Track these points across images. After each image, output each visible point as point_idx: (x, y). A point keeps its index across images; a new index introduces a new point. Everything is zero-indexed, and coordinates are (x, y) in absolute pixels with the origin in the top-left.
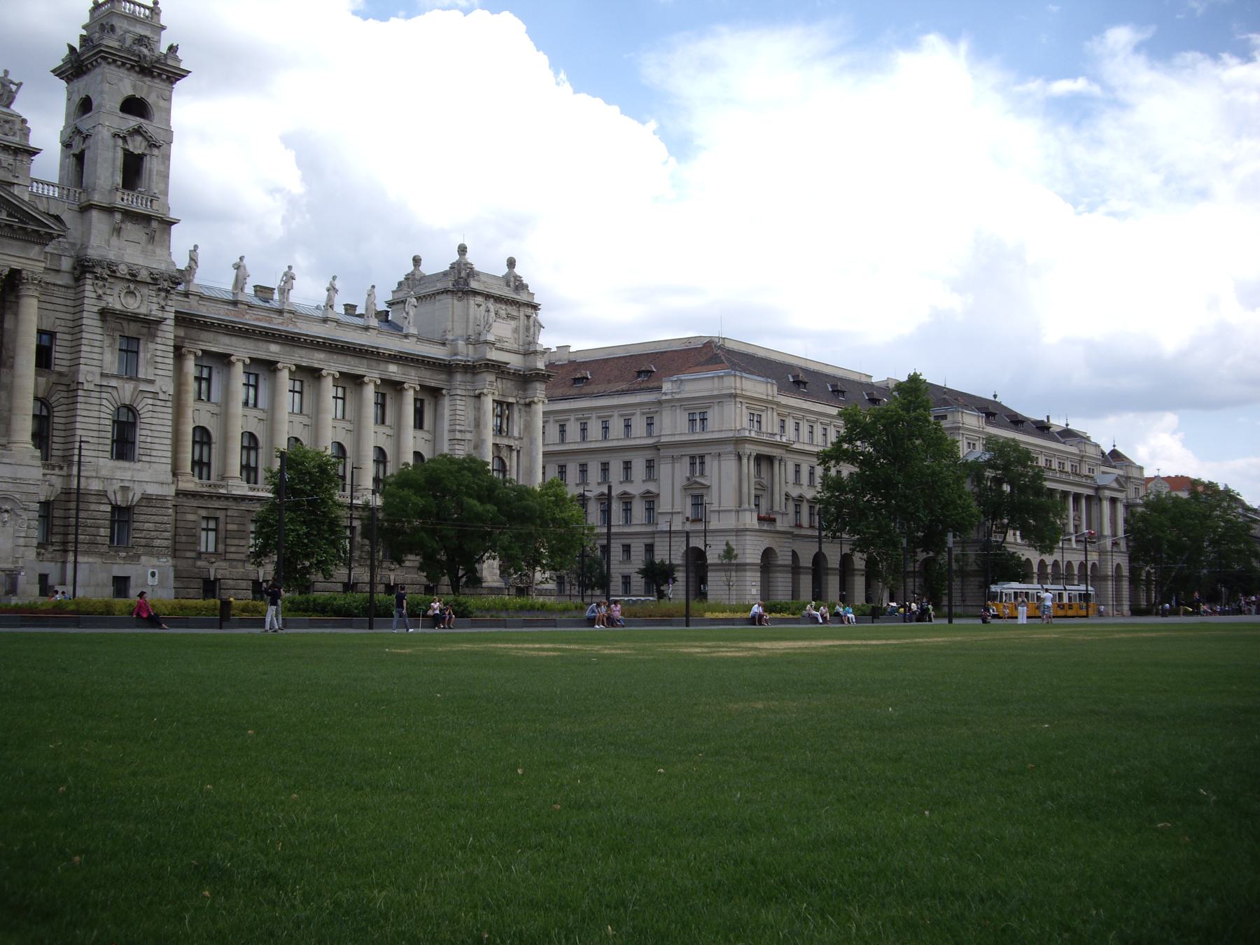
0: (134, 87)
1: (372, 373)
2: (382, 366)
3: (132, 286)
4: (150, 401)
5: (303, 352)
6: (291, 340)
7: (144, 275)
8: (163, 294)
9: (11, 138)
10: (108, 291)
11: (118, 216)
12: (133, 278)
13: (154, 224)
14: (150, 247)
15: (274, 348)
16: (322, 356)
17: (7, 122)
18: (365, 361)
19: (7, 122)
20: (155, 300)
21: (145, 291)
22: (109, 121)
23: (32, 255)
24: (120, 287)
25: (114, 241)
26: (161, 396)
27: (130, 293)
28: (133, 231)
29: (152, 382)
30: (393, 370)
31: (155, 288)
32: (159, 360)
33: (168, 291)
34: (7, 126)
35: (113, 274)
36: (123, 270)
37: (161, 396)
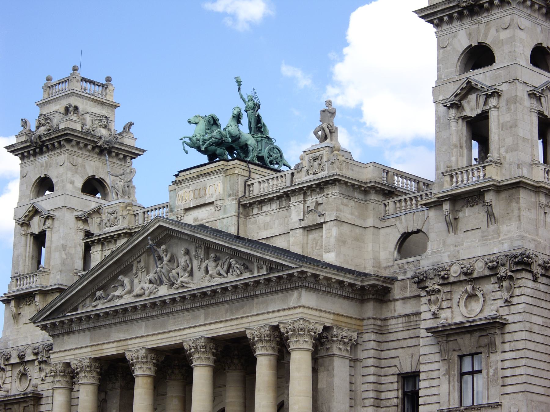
0: (470, 35)
3: (469, 288)
7: (480, 269)
8: (505, 284)
9: (321, 175)
10: (445, 304)
11: (447, 206)
12: (469, 277)
13: (489, 197)
14: (492, 227)
17: (315, 159)
19: (315, 159)
20: (498, 295)
21: (489, 287)
23: (292, 305)
24: (459, 292)
25: (451, 238)
27: (472, 296)
28: (471, 216)
31: (493, 280)
32: (508, 373)
33: (511, 278)
34: (316, 164)
35: (445, 281)
36: (455, 272)
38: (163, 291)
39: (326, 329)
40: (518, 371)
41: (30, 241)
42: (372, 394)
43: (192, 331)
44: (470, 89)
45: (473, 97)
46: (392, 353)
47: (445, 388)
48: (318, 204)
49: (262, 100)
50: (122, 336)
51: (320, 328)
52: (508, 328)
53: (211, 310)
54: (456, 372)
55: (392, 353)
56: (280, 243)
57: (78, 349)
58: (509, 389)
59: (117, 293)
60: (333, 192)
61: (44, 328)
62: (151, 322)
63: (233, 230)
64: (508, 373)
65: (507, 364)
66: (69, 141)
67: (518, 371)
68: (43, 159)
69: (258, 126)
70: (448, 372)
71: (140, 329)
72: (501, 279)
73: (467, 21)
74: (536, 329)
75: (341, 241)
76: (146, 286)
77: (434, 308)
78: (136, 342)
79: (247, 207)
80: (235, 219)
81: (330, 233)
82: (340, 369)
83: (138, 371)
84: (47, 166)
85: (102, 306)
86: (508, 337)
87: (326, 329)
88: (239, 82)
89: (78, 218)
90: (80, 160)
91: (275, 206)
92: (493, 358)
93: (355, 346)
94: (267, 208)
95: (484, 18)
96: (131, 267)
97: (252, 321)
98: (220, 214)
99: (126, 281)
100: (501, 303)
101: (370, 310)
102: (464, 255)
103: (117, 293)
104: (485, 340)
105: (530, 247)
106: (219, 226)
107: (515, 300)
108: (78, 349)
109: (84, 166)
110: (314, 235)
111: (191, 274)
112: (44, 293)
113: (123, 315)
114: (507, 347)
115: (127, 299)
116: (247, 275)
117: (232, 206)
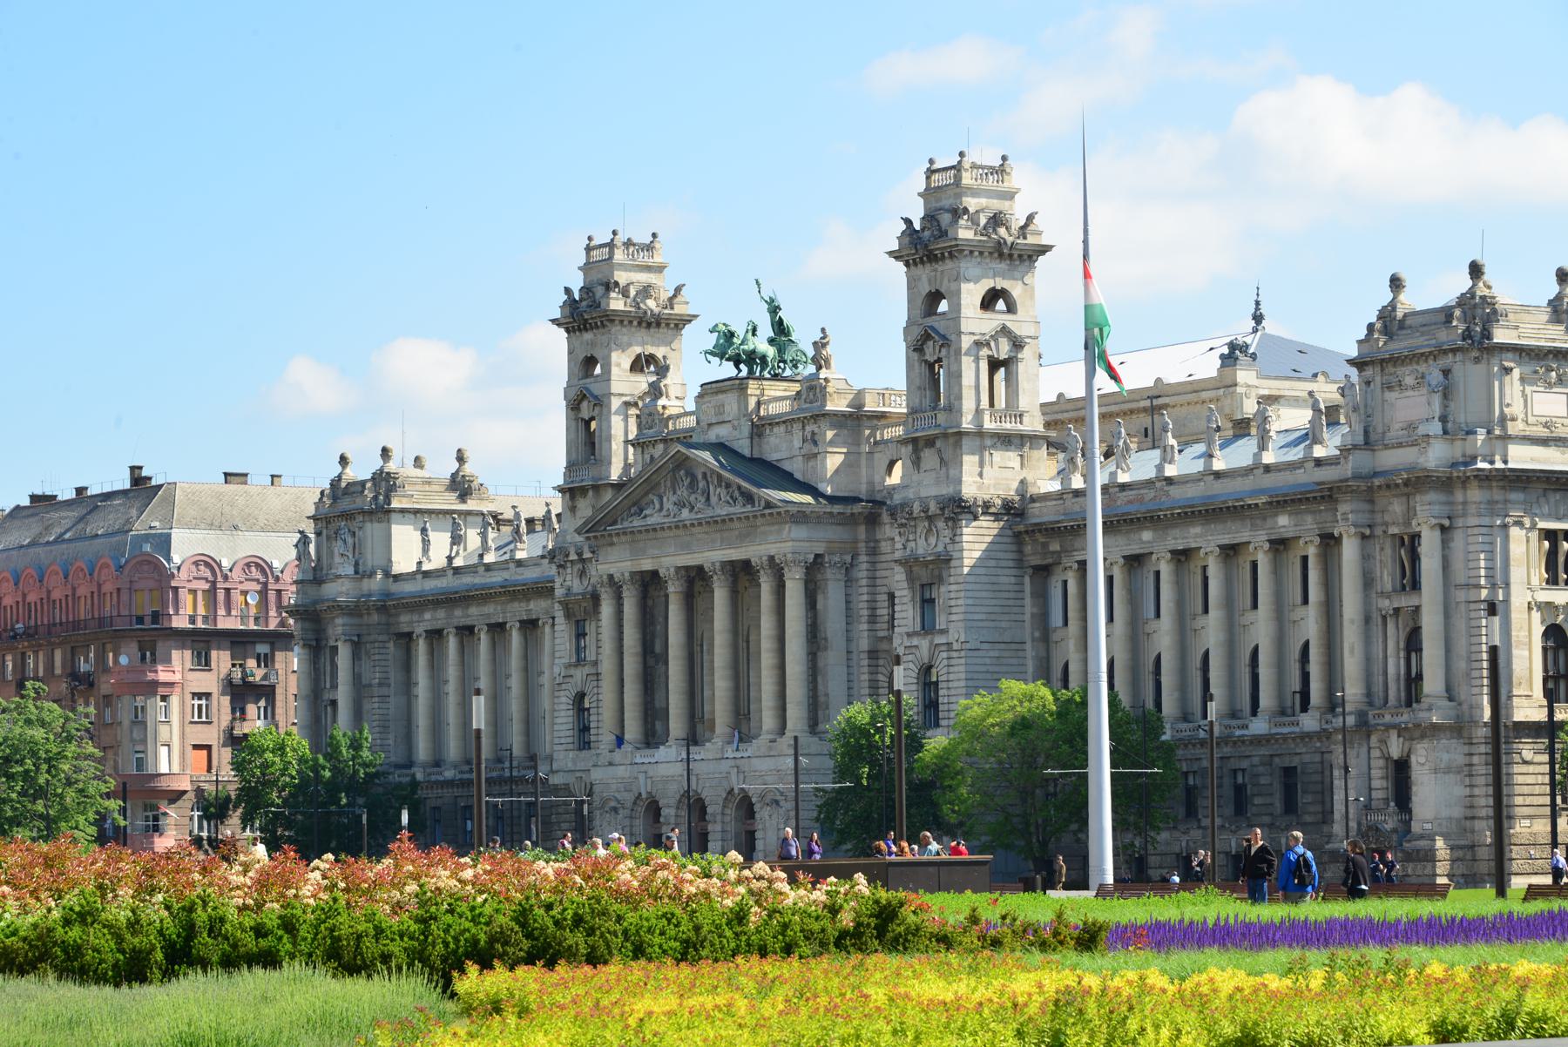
1: (1257, 538)
4: (944, 655)
5: (1176, 532)
6: (1152, 519)
13: (938, 444)
15: (1147, 535)
16: (1197, 530)
18: (1248, 522)
26: (955, 646)
27: (930, 530)
29: (944, 632)
30: (1284, 522)
32: (953, 603)
35: (911, 517)
39: (817, 556)
40: (960, 602)
43: (712, 555)
47: (911, 612)
48: (813, 433)
49: (780, 301)
56: (786, 466)
58: (954, 617)
63: (747, 452)
64: (953, 603)
65: (953, 595)
66: (612, 321)
67: (960, 602)
69: (780, 328)
70: (913, 599)
78: (669, 559)
80: (748, 442)
83: (671, 589)
84: (593, 344)
87: (817, 556)
91: (783, 428)
92: (943, 589)
93: (849, 569)
95: (940, 267)
96: (658, 484)
97: (755, 551)
98: (736, 433)
100: (947, 540)
102: (923, 494)
103: (647, 512)
106: (736, 446)
108: (618, 562)
111: (708, 499)
114: (952, 580)
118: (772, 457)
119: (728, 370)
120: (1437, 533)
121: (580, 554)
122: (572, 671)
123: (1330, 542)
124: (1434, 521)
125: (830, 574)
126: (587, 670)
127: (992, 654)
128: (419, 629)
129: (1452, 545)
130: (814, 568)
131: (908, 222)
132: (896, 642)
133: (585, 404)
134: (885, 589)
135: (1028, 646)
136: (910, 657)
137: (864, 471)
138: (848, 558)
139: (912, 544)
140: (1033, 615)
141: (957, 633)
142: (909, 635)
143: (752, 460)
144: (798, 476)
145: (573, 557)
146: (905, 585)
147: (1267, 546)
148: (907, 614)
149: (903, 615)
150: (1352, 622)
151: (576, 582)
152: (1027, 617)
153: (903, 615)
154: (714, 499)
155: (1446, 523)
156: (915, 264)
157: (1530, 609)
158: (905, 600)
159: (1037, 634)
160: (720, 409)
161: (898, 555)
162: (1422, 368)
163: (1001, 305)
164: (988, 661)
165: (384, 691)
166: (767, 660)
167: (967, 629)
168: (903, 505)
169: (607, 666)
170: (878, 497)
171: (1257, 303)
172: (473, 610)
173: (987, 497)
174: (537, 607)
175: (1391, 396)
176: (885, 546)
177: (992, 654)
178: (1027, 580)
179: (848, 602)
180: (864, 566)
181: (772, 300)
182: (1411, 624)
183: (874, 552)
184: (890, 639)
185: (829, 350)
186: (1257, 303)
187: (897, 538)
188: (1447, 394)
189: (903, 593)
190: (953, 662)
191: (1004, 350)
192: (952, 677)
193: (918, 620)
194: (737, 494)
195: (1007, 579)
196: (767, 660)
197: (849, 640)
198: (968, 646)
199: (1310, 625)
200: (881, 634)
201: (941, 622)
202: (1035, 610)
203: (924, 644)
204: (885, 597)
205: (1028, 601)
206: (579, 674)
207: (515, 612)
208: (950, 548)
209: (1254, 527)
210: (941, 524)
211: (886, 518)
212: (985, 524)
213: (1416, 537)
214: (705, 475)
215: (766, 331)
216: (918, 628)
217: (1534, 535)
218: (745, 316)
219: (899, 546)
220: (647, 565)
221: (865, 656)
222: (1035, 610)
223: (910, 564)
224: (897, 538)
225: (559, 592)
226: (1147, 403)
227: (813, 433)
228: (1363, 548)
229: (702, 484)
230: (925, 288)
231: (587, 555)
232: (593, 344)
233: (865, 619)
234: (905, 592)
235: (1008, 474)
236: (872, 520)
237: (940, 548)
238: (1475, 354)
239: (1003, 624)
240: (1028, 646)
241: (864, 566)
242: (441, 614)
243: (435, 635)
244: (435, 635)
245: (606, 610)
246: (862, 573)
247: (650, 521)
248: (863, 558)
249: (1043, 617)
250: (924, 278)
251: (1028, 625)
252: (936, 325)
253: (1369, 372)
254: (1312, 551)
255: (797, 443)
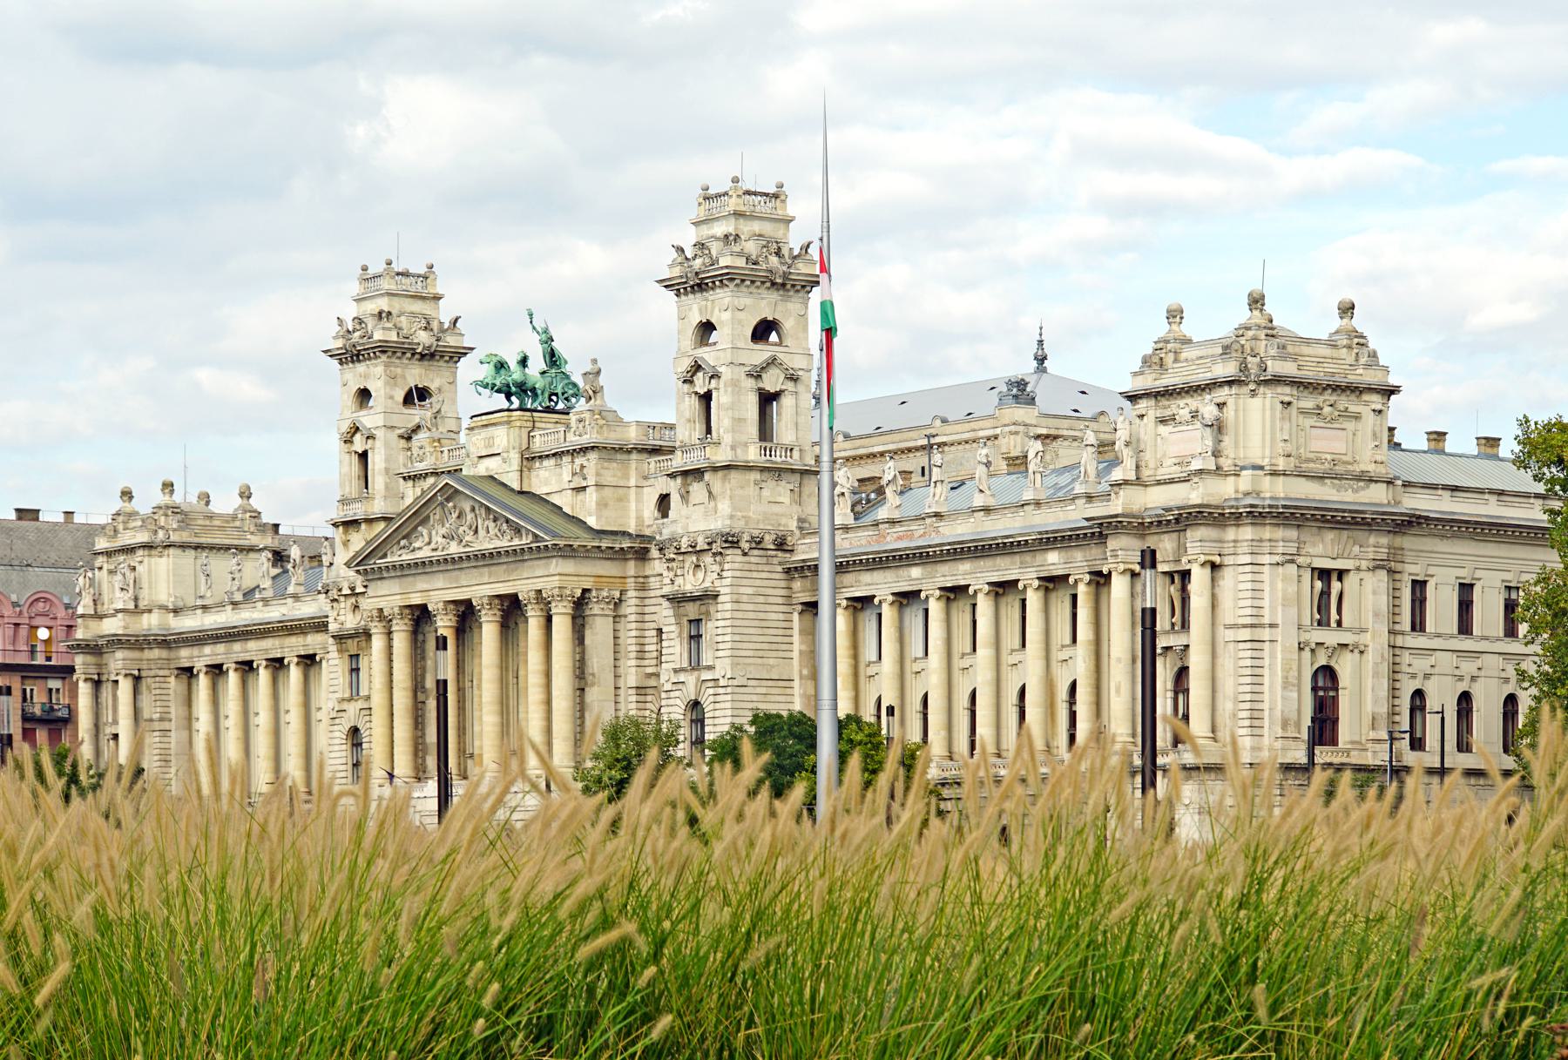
1: (1025, 571)
2: (1039, 558)
4: (711, 691)
5: (944, 568)
11: (679, 480)
13: (707, 476)
15: (916, 572)
18: (1017, 558)
21: (708, 559)
22: (731, 347)
30: (1054, 561)
32: (720, 639)
37: (722, 683)
38: (454, 549)
39: (585, 591)
40: (727, 638)
41: (355, 459)
42: (634, 648)
43: (480, 587)
44: (697, 367)
45: (700, 374)
46: (652, 609)
47: (677, 650)
48: (582, 467)
50: (426, 586)
51: (578, 593)
52: (720, 599)
53: (493, 568)
54: (685, 635)
55: (652, 609)
56: (555, 499)
57: (390, 596)
58: (720, 654)
59: (417, 545)
60: (593, 456)
61: (358, 572)
62: (447, 575)
63: (516, 486)
64: (720, 639)
65: (720, 631)
67: (727, 638)
68: (361, 368)
69: (553, 358)
70: (680, 635)
71: (439, 581)
72: (715, 554)
73: (698, 295)
74: (745, 598)
75: (602, 504)
76: (440, 540)
77: (671, 574)
78: (437, 592)
79: (530, 459)
81: (591, 496)
82: (599, 631)
84: (366, 376)
85: (407, 557)
86: (720, 607)
87: (585, 591)
88: (531, 315)
89: (401, 437)
90: (399, 371)
91: (552, 461)
92: (710, 624)
93: (618, 603)
94: (546, 463)
95: (710, 295)
96: (428, 517)
99: (425, 532)
100: (715, 575)
101: (631, 568)
103: (417, 545)
104: (703, 609)
105: (738, 526)
107: (725, 574)
108: (390, 596)
109: (404, 377)
110: (581, 496)
111: (476, 532)
112: (369, 521)
113: (422, 567)
114: (719, 616)
115: (425, 553)
116: (516, 542)
117: (515, 457)
118: (540, 490)
119: (500, 401)
120: (1208, 570)
121: (352, 589)
122: (345, 706)
123: (1101, 580)
124: (1203, 558)
125: (595, 609)
126: (361, 704)
127: (759, 690)
128: (199, 665)
129: (1221, 583)
130: (580, 603)
131: (680, 250)
132: (663, 678)
133: (358, 437)
134: (653, 625)
135: (796, 684)
136: (677, 694)
137: (633, 506)
138: (617, 594)
139: (679, 581)
140: (801, 652)
141: (723, 668)
142: (676, 671)
143: (521, 493)
144: (567, 510)
145: (346, 591)
146: (673, 620)
147: (1036, 583)
148: (676, 650)
149: (671, 650)
150: (1119, 660)
151: (350, 616)
152: (795, 654)
153: (671, 650)
154: (482, 532)
155: (1217, 559)
156: (686, 294)
157: (1300, 649)
158: (673, 636)
159: (805, 672)
160: (490, 441)
161: (667, 590)
162: (1193, 402)
163: (773, 337)
164: (755, 698)
165: (166, 725)
166: (534, 694)
167: (734, 666)
168: (672, 540)
169: (378, 701)
170: (647, 532)
171: (1041, 342)
172: (252, 645)
173: (756, 533)
174: (313, 642)
175: (1162, 429)
176: (653, 582)
177: (759, 690)
178: (796, 616)
179: (615, 638)
180: (633, 601)
181: (546, 331)
182: (1179, 664)
183: (643, 587)
184: (657, 675)
185: (602, 380)
186: (1041, 342)
187: (665, 573)
188: (1218, 427)
189: (671, 629)
190: (718, 698)
191: (771, 382)
192: (717, 713)
193: (686, 655)
194: (505, 526)
195: (775, 616)
196: (534, 694)
197: (616, 676)
198: (735, 682)
199: (1080, 668)
200: (650, 670)
201: (707, 660)
202: (804, 647)
203: (690, 679)
204: (654, 633)
205: (796, 638)
206: (353, 708)
207: (291, 648)
208: (717, 583)
209: (1023, 565)
210: (708, 559)
211: (654, 553)
212: (753, 560)
213: (1185, 575)
214: (473, 509)
215: (537, 364)
216: (685, 664)
217: (1307, 575)
218: (519, 343)
219: (667, 581)
220: (416, 600)
221: (633, 691)
222: (804, 647)
223: (678, 600)
224: (665, 573)
225: (333, 627)
226: (925, 442)
227: (582, 467)
228: (1132, 586)
229: (470, 516)
230: (696, 318)
231: (359, 589)
232: (366, 376)
233: (633, 655)
234: (673, 628)
235: (776, 509)
236: (642, 555)
237: (707, 584)
238: (1252, 386)
239: (771, 661)
240: (796, 684)
241: (633, 601)
242: (221, 648)
243: (217, 670)
244: (217, 670)
245: (378, 643)
246: (629, 608)
247: (419, 554)
248: (631, 593)
249: (812, 656)
250: (695, 308)
251: (796, 662)
252: (706, 356)
253: (1143, 404)
254: (1082, 590)
255: (566, 476)
